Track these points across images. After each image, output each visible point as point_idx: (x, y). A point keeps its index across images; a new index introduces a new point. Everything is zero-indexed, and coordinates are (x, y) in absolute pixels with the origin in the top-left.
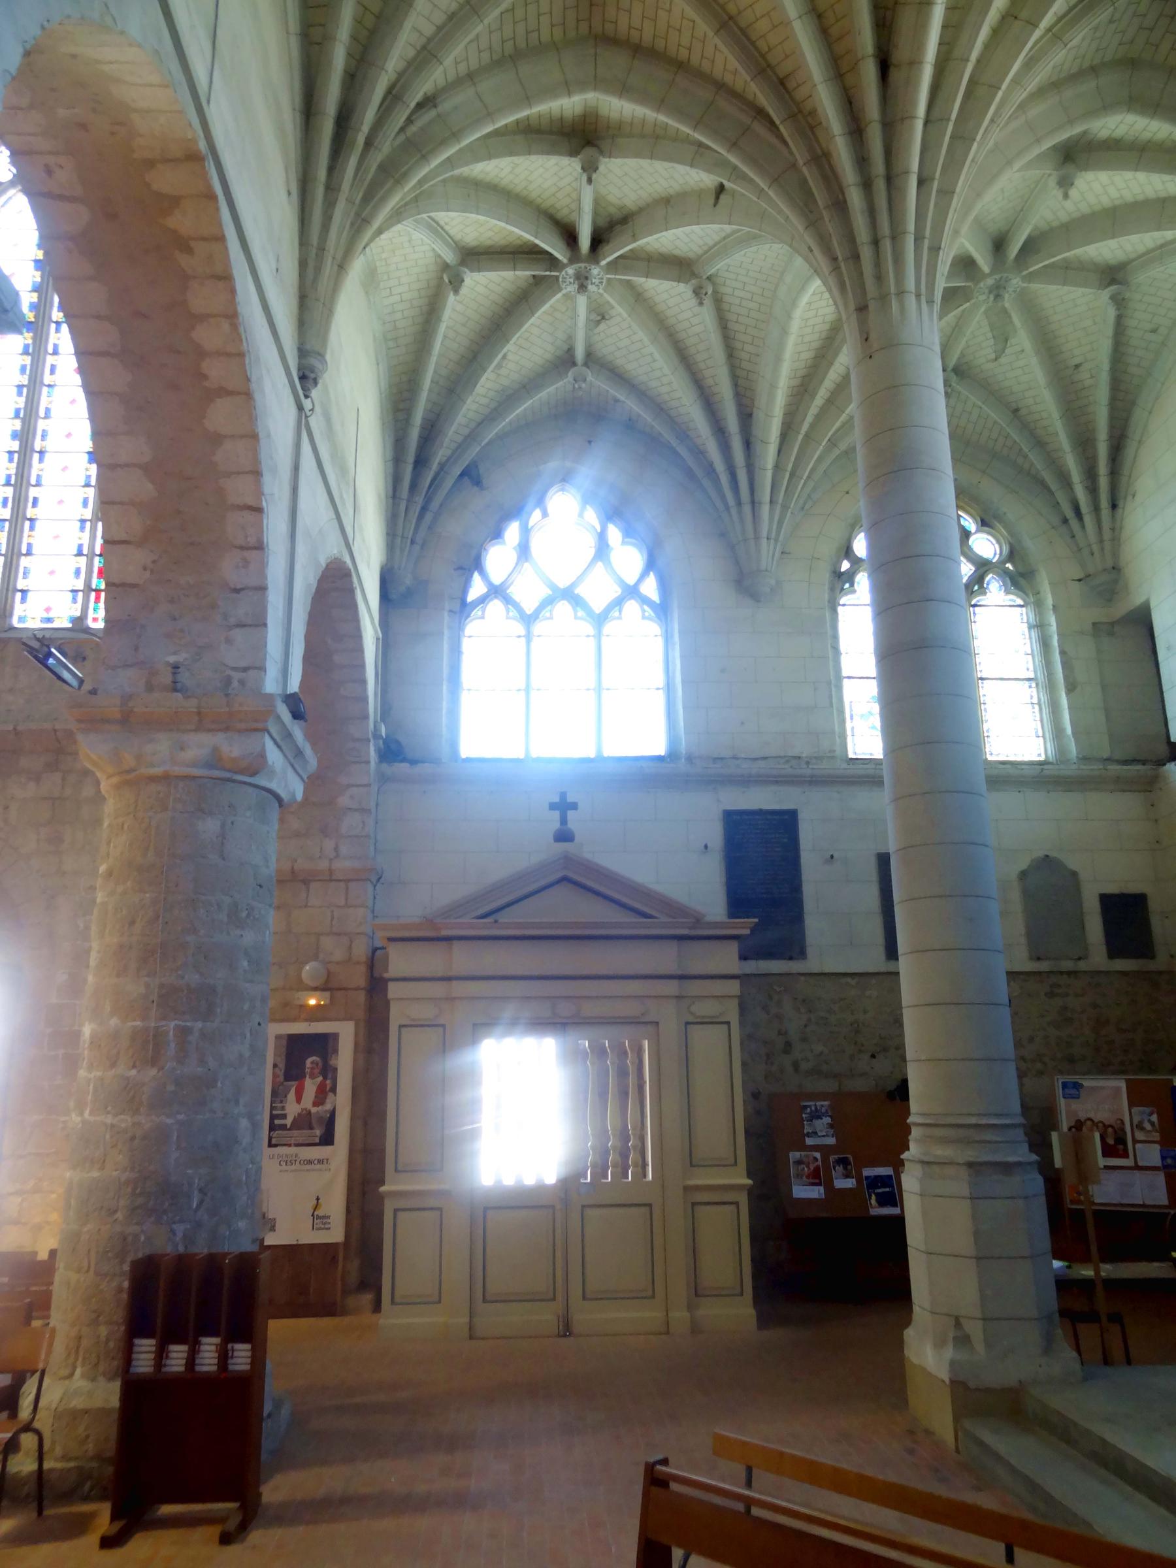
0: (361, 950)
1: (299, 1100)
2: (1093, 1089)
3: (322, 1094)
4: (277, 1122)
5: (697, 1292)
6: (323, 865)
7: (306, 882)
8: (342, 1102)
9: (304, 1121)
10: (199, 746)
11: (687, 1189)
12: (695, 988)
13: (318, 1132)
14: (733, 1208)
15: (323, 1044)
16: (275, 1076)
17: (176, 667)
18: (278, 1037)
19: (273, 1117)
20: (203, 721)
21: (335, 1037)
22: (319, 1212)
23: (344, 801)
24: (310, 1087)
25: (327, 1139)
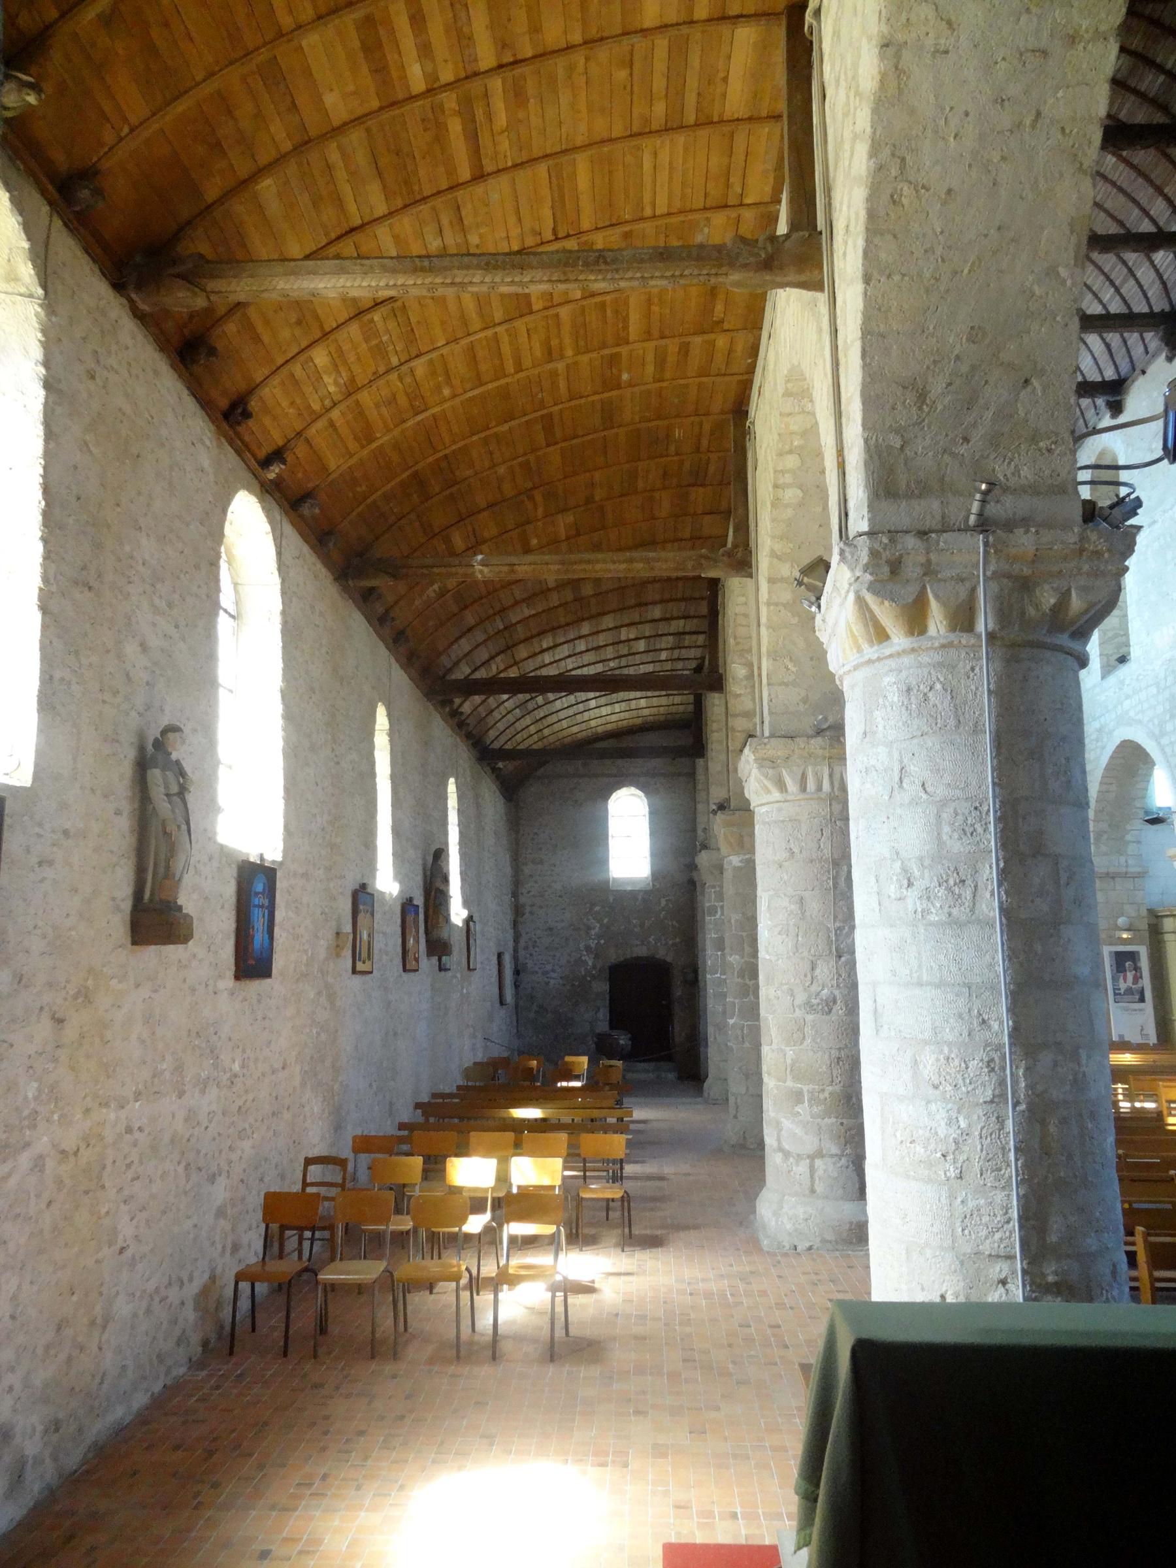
0: (1144, 913)
1: (1125, 982)
3: (1136, 979)
6: (1124, 870)
7: (1113, 878)
8: (1146, 982)
9: (1129, 991)
13: (1137, 997)
15: (1133, 956)
16: (1112, 970)
18: (1110, 953)
19: (1114, 989)
21: (1138, 953)
22: (1144, 1032)
23: (1128, 837)
25: (1142, 1000)
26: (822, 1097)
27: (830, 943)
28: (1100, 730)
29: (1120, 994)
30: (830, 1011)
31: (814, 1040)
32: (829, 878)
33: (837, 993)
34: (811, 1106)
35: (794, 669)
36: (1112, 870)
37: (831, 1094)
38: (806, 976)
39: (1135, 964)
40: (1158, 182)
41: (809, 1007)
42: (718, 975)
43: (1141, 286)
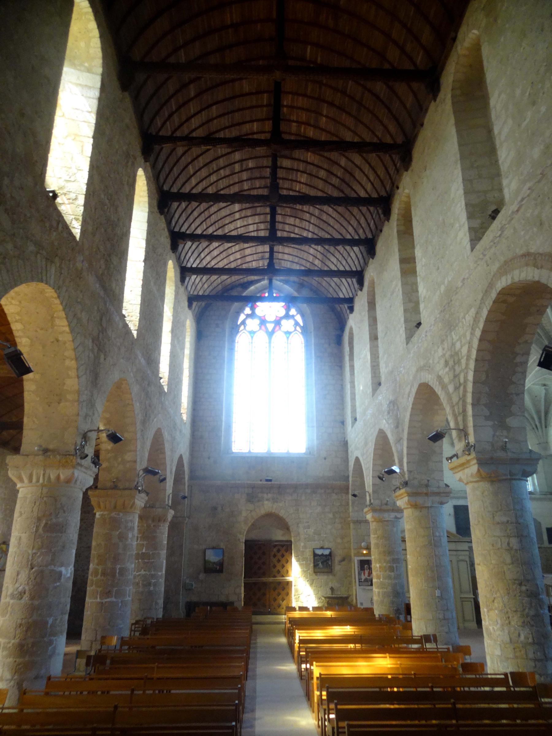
1: (364, 575)
2: (546, 577)
4: (360, 580)
5: (464, 620)
7: (360, 523)
9: (366, 580)
10: (393, 515)
11: (461, 598)
12: (459, 553)
13: (370, 583)
14: (470, 603)
16: (358, 569)
17: (387, 501)
18: (358, 560)
20: (393, 511)
24: (367, 572)
26: (9, 645)
27: (28, 561)
28: (351, 452)
29: (362, 582)
30: (21, 598)
31: (11, 614)
32: (34, 527)
33: (27, 588)
34: (2, 652)
35: (37, 422)
36: (360, 519)
37: (13, 644)
38: (14, 579)
39: (369, 566)
40: (348, 219)
41: (12, 596)
42: (135, 573)
43: (352, 260)
